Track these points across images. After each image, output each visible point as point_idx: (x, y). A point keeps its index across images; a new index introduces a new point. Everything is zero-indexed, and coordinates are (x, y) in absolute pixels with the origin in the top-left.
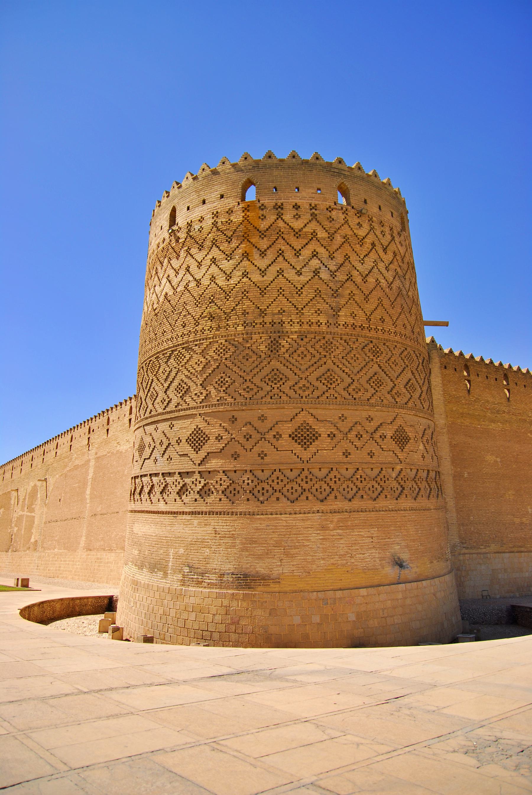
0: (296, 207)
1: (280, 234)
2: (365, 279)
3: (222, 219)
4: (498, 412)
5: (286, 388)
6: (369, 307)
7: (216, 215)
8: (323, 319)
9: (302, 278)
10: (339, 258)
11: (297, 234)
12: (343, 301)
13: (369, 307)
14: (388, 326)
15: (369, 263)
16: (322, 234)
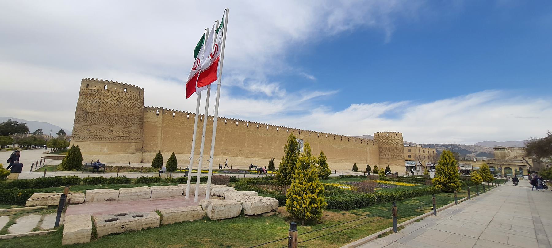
0: (95, 90)
1: (91, 95)
2: (107, 103)
3: (83, 91)
4: (183, 123)
5: (87, 122)
6: (106, 108)
7: (83, 90)
8: (96, 111)
9: (93, 103)
10: (102, 99)
11: (94, 95)
12: (100, 107)
13: (106, 108)
14: (112, 111)
15: (109, 100)
16: (99, 95)
